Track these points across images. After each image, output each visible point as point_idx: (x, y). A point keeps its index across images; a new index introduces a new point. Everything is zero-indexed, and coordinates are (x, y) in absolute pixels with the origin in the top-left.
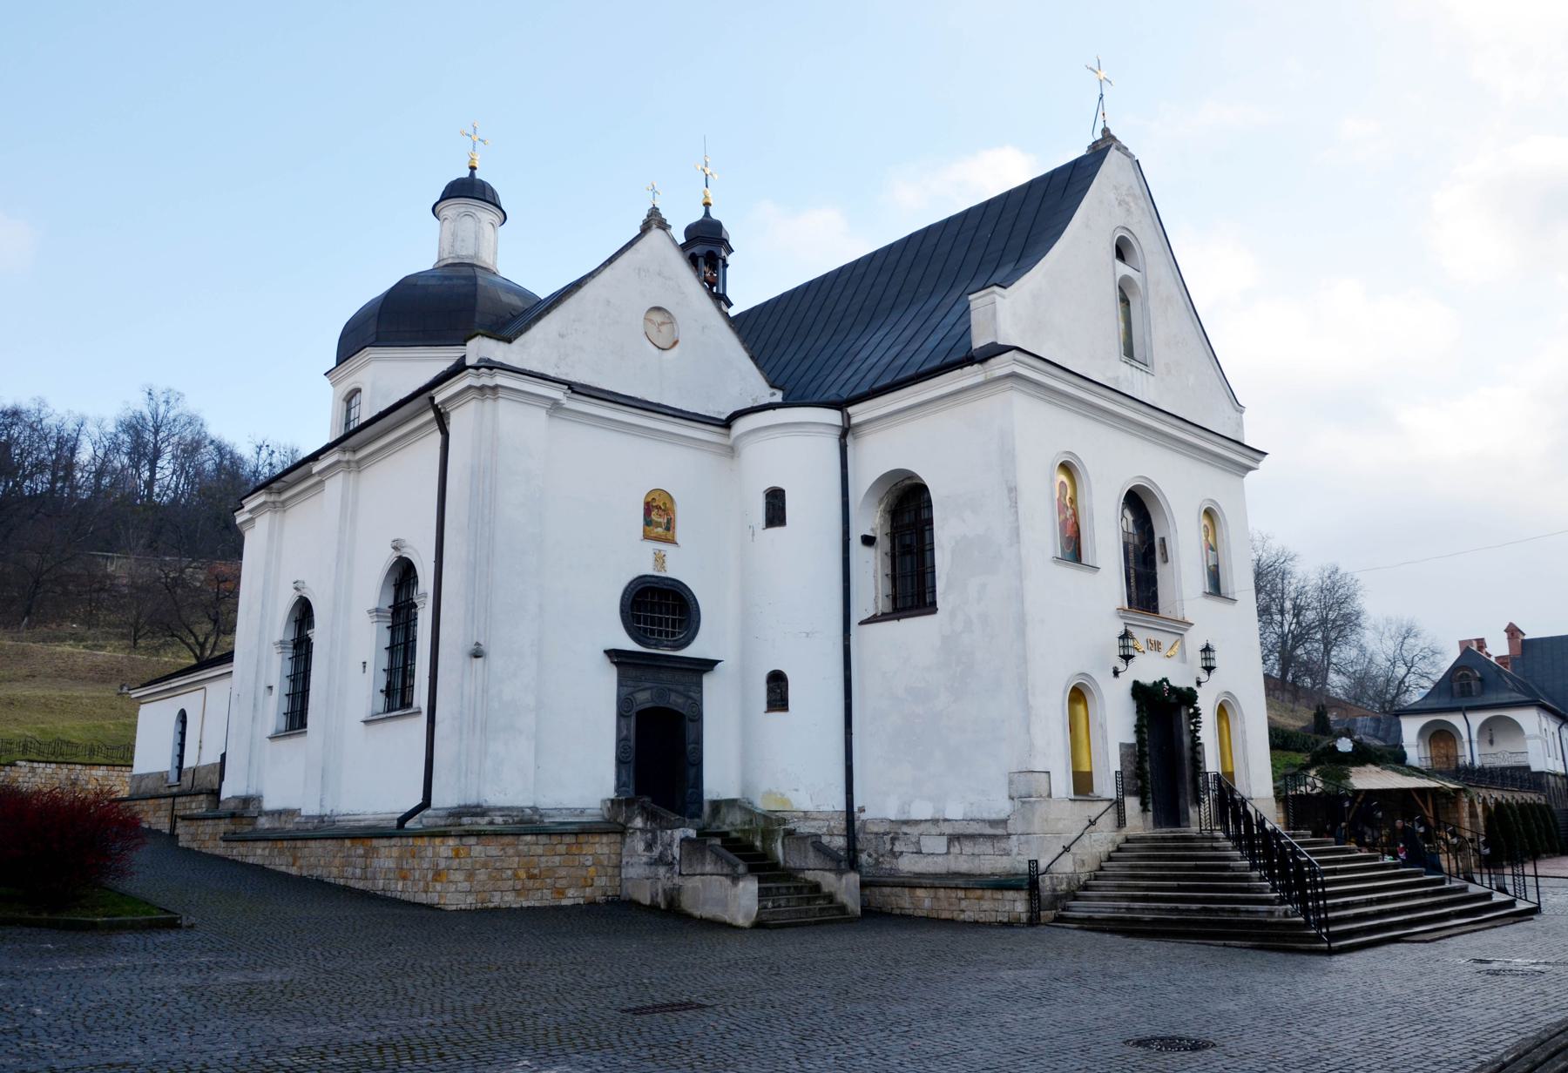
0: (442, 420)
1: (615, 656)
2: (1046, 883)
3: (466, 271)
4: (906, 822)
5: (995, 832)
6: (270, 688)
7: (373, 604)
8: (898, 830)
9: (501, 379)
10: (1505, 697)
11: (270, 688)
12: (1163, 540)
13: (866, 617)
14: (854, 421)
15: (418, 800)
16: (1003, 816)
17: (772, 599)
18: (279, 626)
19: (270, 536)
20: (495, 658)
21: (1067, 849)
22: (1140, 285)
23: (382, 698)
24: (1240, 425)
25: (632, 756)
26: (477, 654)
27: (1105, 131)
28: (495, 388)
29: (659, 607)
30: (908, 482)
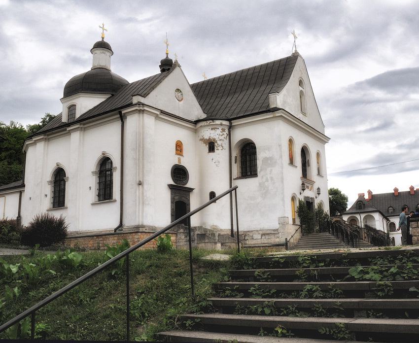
0: (122, 118)
1: (170, 186)
2: (288, 245)
3: (106, 71)
4: (248, 231)
5: (275, 232)
6: (46, 195)
7: (95, 170)
8: (246, 233)
9: (146, 108)
10: (370, 209)
11: (46, 195)
12: (308, 160)
14: (233, 124)
15: (117, 224)
16: (277, 228)
17: (213, 172)
18: (48, 175)
19: (44, 149)
20: (145, 186)
21: (292, 237)
22: (304, 92)
23: (97, 198)
24: (324, 131)
25: (174, 214)
26: (140, 184)
28: (143, 111)
29: (179, 173)
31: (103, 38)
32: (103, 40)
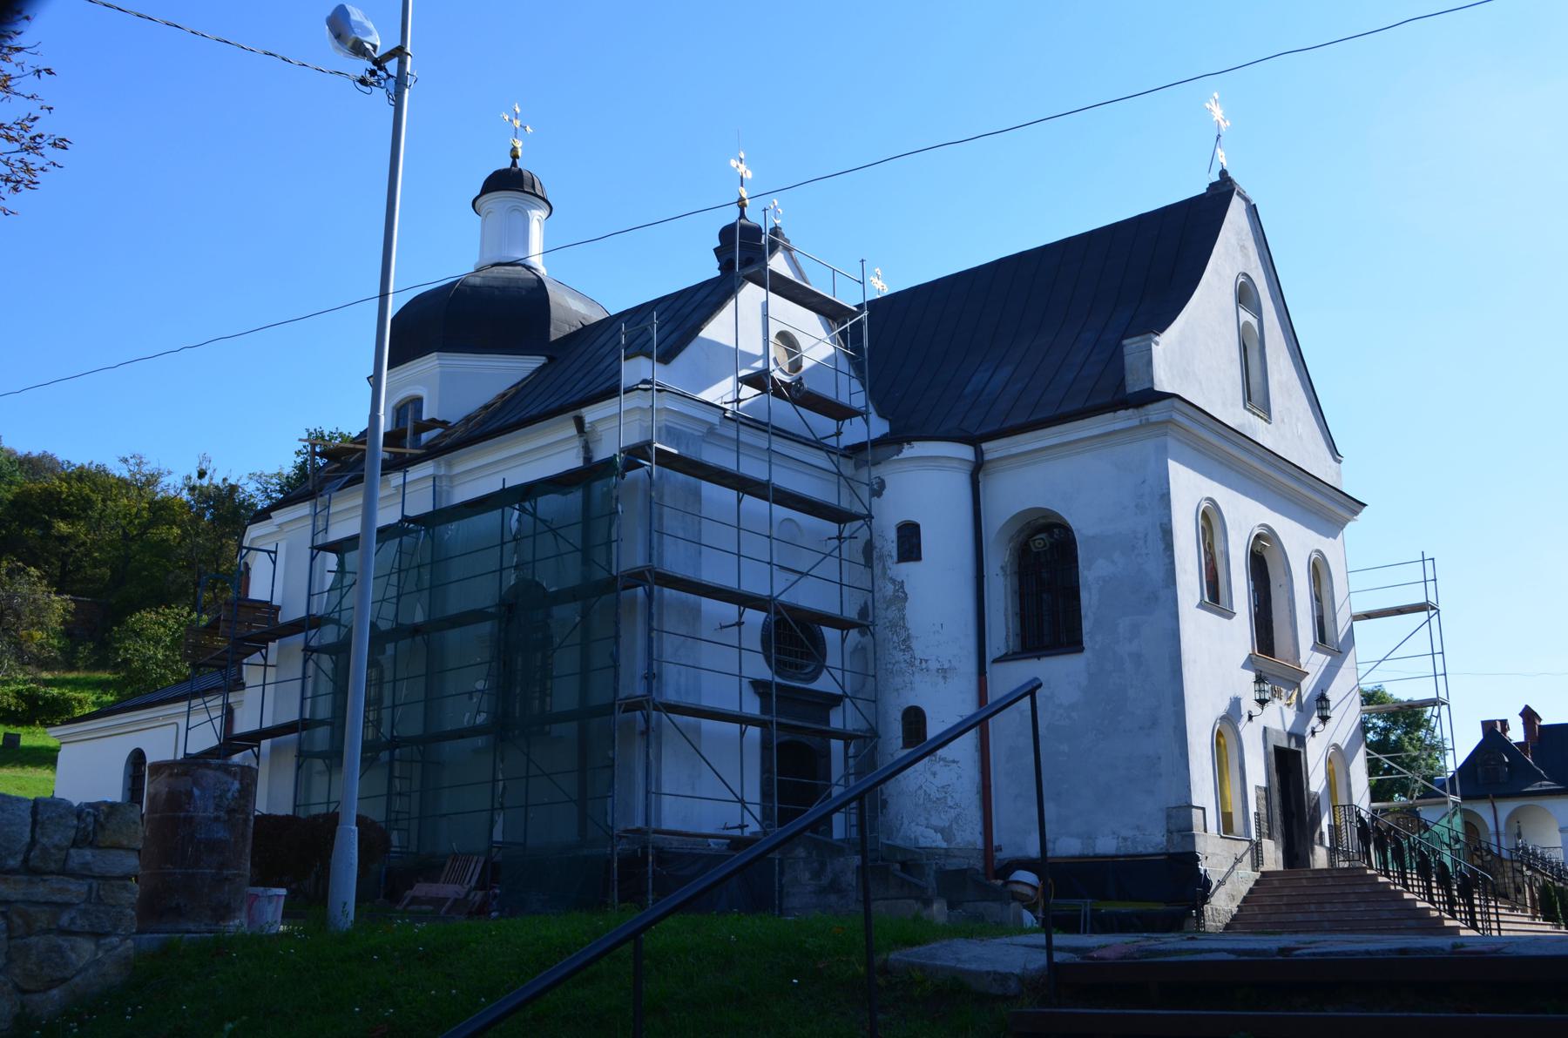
13: (998, 654)
14: (987, 457)
24: (1339, 474)
27: (1223, 173)
30: (1042, 521)
31: (515, 157)
32: (514, 164)
